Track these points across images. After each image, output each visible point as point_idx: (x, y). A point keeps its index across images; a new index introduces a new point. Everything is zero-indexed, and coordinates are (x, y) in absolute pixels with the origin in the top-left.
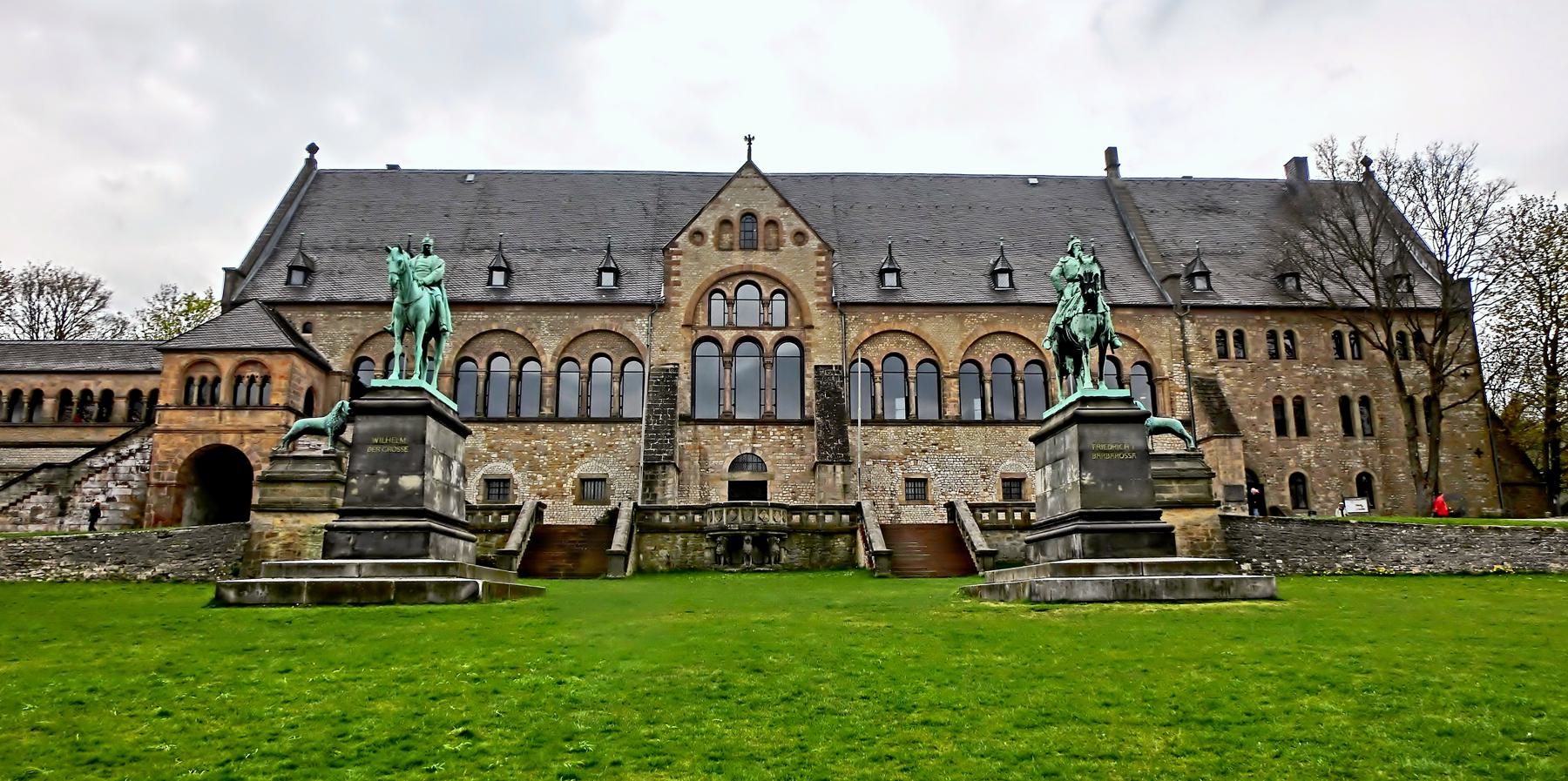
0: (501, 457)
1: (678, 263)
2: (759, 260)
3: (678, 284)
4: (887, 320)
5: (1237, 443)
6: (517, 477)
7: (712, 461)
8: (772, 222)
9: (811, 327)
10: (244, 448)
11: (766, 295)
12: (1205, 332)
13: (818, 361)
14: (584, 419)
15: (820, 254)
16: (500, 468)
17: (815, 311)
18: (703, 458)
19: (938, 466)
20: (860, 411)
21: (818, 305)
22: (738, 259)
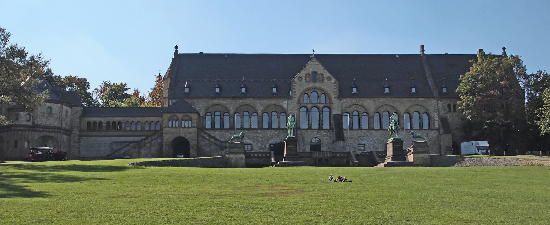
0: (249, 139)
2: (318, 85)
3: (295, 92)
4: (354, 101)
5: (450, 135)
6: (253, 144)
7: (306, 140)
10: (187, 137)
11: (320, 94)
13: (334, 113)
14: (270, 128)
17: (333, 99)
18: (304, 139)
20: (346, 125)
22: (312, 85)
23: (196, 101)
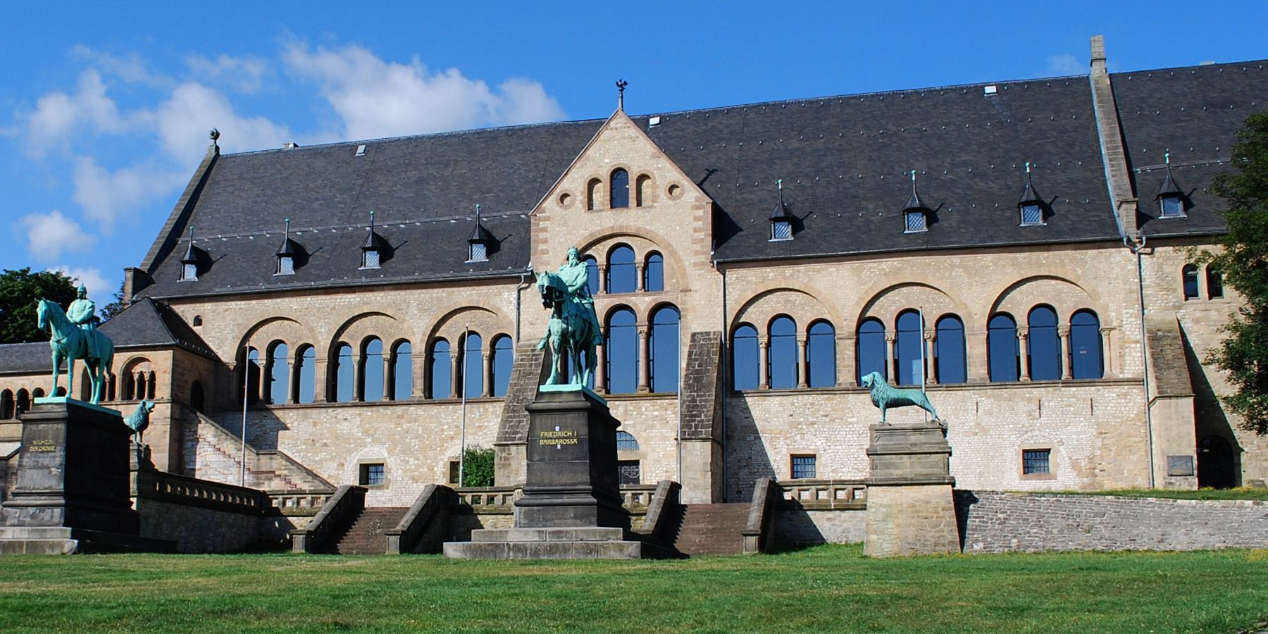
0: (376, 441)
1: (545, 230)
2: (628, 219)
3: (545, 252)
8: (642, 178)
9: (686, 291)
12: (1167, 269)
15: (698, 208)
16: (372, 454)
17: (691, 271)
19: (827, 439)
21: (695, 264)
22: (608, 220)
23: (206, 309)
